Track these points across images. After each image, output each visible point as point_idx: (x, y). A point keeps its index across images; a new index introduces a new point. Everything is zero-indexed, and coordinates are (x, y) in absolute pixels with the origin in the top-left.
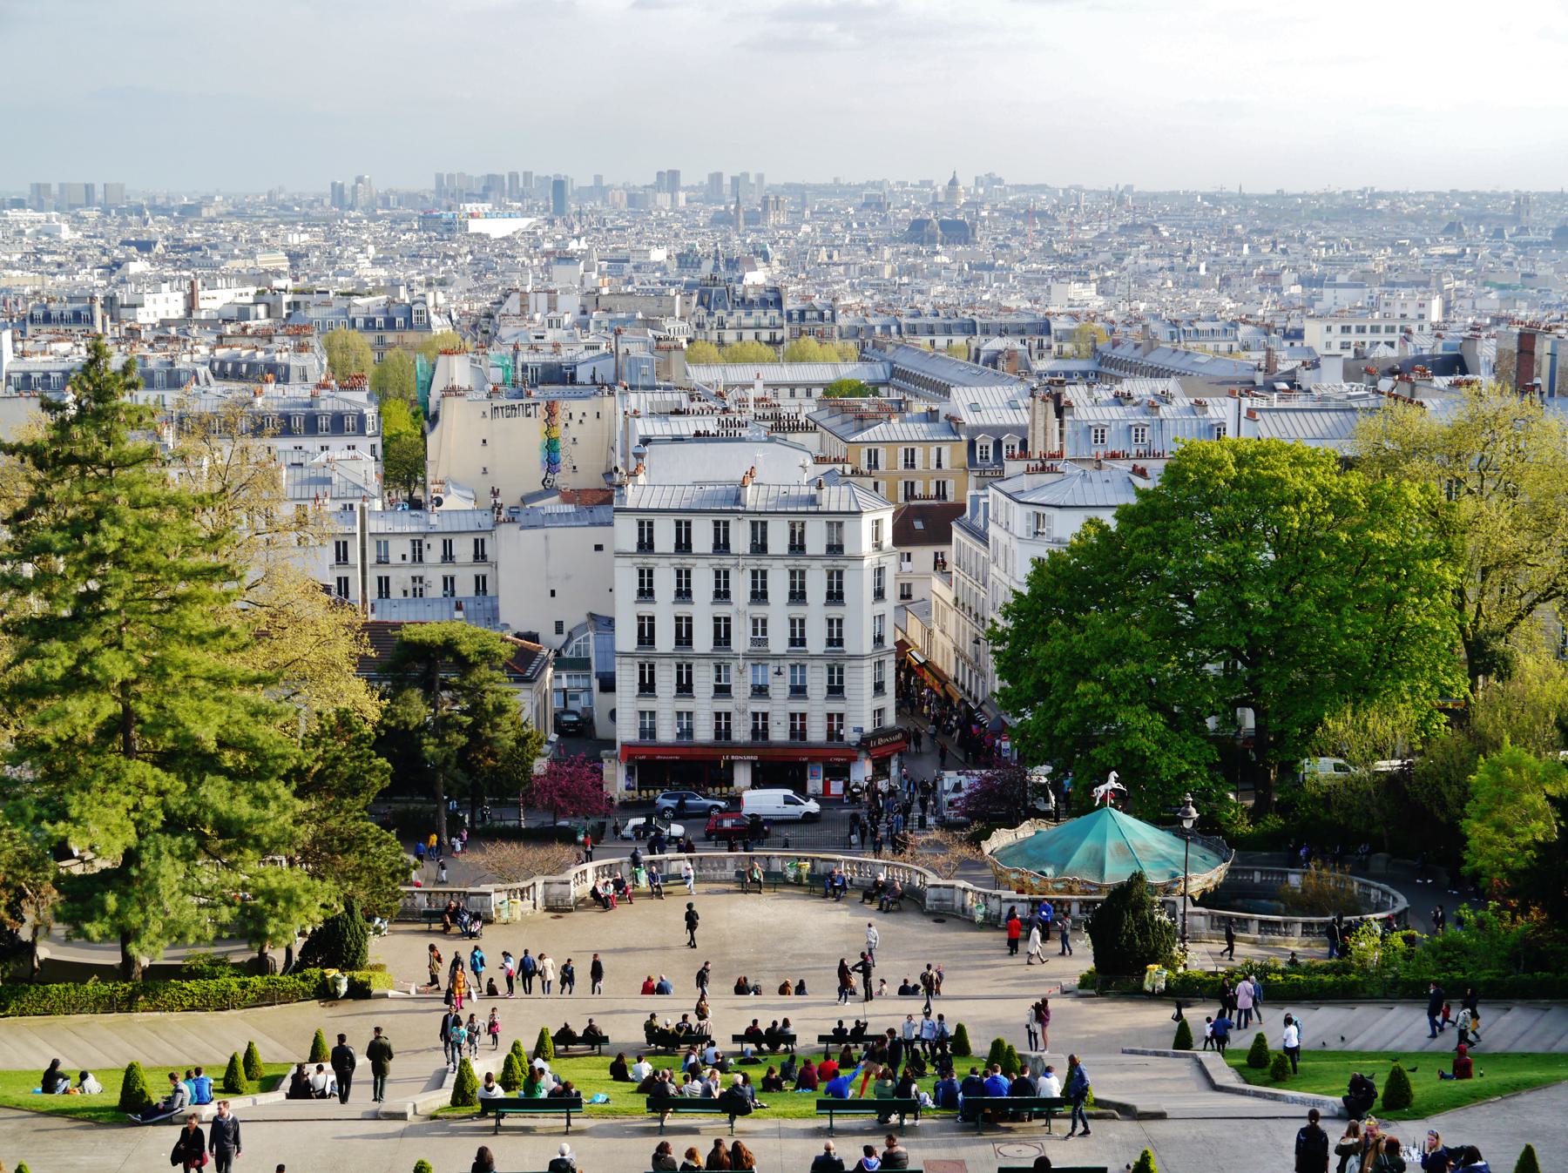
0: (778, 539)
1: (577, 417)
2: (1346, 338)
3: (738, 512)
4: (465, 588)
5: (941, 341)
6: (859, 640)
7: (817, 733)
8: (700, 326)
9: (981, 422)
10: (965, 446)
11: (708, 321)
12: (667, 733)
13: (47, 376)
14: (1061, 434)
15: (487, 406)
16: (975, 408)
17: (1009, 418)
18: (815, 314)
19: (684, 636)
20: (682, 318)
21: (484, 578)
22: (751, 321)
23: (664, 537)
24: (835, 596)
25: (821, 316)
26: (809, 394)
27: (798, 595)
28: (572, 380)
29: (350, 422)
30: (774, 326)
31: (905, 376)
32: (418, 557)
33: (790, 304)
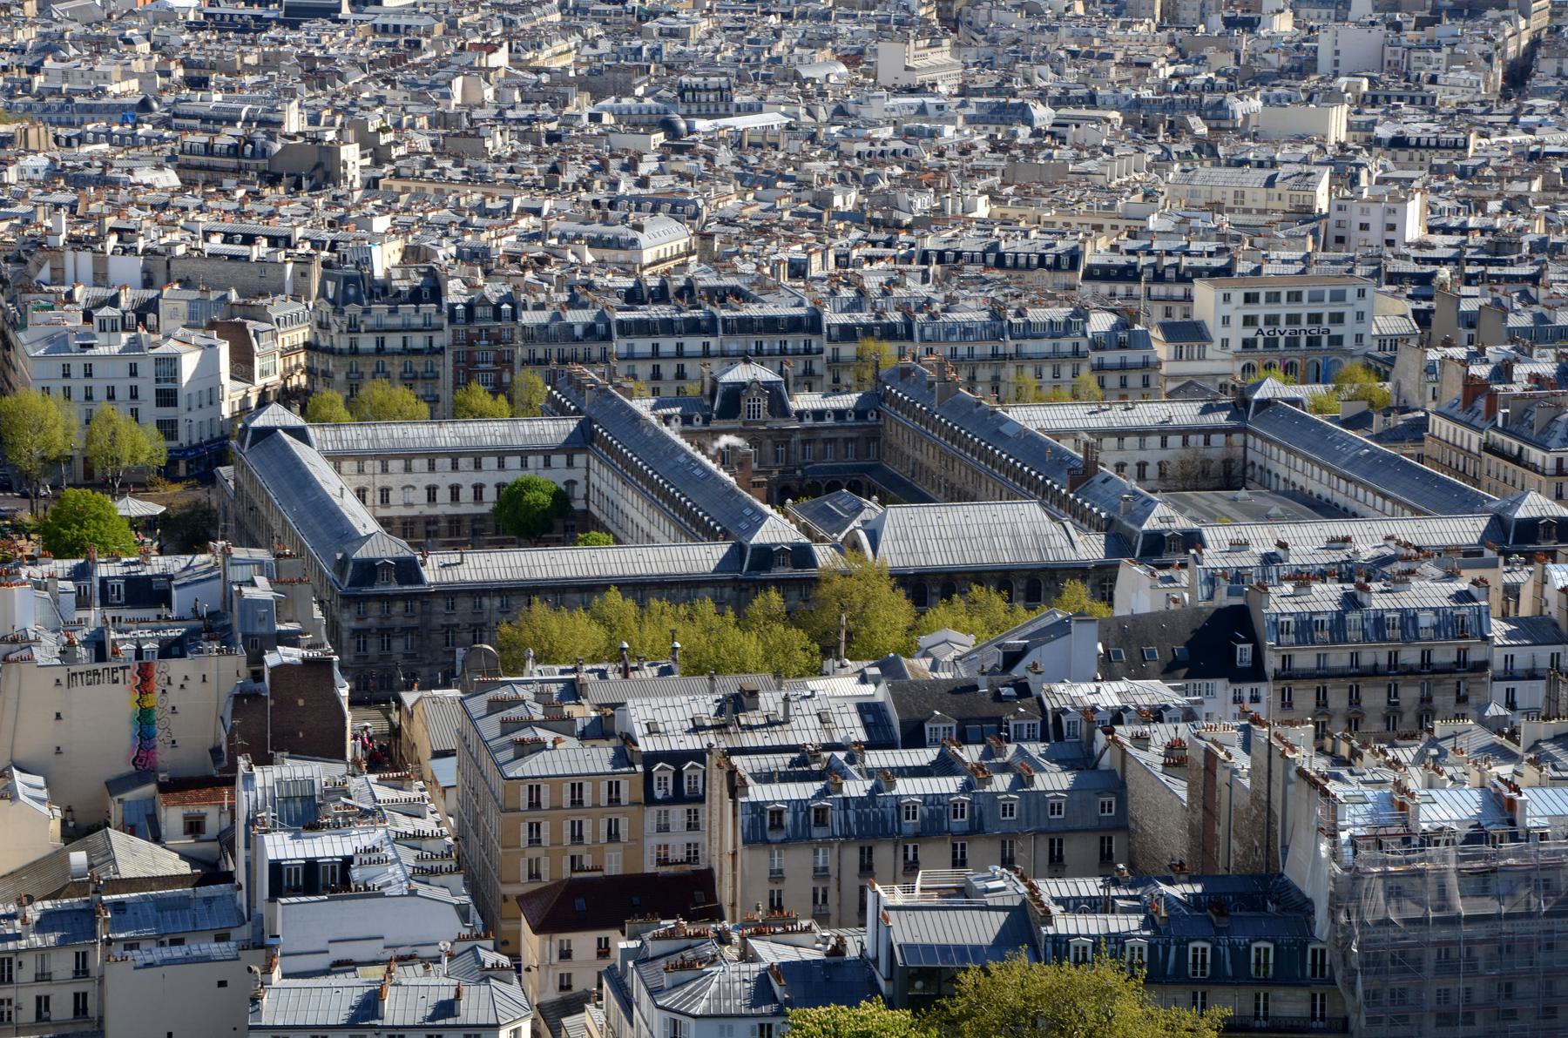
1: (177, 681)
2: (1251, 310)
3: (375, 1026)
4: (62, 1007)
5: (668, 345)
8: (323, 326)
9: (659, 748)
10: (640, 780)
14: (735, 815)
15: (62, 674)
16: (652, 730)
17: (693, 743)
18: (489, 312)
20: (296, 297)
21: (85, 995)
22: (396, 321)
25: (497, 309)
26: (478, 466)
30: (429, 328)
33: (455, 291)
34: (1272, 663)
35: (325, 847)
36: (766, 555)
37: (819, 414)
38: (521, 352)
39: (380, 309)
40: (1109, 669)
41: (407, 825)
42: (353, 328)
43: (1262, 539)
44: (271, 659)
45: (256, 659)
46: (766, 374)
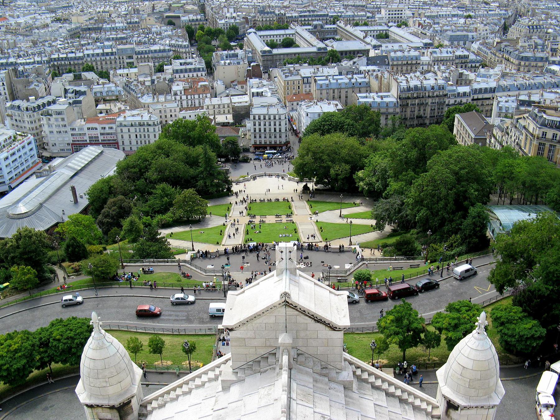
0: (272, 118)
5: (306, 19)
6: (283, 130)
7: (278, 143)
11: (260, 17)
12: (258, 143)
13: (142, 51)
19: (260, 130)
23: (257, 118)
24: (280, 125)
27: (275, 125)
28: (237, 56)
29: (201, 69)
30: (273, 17)
31: (298, 33)
32: (219, 108)
34: (391, 63)
35: (260, 90)
36: (319, 49)
37: (328, 28)
38: (286, 20)
39: (266, 15)
40: (368, 64)
41: (270, 87)
42: (262, 17)
43: (390, 46)
44: (252, 64)
45: (249, 64)
46: (320, 23)
